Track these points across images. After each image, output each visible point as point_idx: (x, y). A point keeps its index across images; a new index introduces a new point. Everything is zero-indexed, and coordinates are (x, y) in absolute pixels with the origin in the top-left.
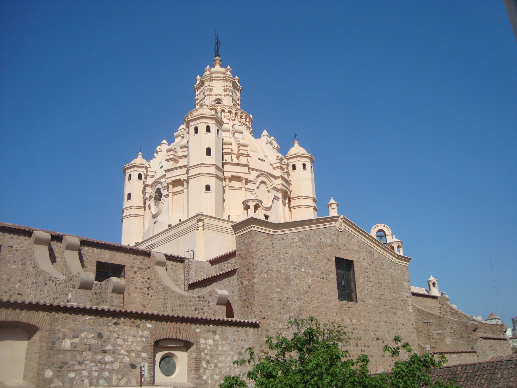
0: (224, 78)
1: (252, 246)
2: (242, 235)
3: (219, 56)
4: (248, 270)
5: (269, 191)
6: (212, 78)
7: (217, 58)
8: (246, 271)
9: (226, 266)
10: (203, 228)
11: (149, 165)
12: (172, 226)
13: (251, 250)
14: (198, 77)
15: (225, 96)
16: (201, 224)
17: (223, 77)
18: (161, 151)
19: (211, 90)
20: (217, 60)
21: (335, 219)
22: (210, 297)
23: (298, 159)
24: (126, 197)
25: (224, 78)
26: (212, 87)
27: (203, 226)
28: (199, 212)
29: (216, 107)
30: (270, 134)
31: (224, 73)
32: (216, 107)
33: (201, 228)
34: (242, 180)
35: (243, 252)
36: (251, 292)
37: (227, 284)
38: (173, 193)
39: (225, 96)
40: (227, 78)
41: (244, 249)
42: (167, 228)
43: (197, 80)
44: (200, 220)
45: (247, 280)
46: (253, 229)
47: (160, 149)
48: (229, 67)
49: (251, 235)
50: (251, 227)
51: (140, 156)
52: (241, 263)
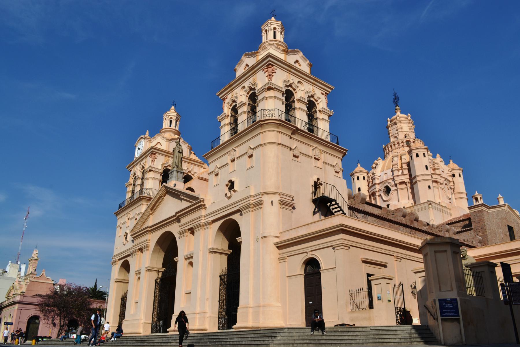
2: (475, 212)
3: (398, 106)
4: (481, 228)
5: (448, 189)
7: (397, 107)
12: (405, 207)
14: (388, 119)
15: (410, 132)
16: (430, 206)
17: (408, 121)
19: (402, 129)
20: (398, 109)
21: (503, 206)
22: (473, 240)
23: (456, 171)
28: (429, 200)
30: (441, 157)
31: (407, 119)
33: (431, 208)
34: (438, 183)
35: (477, 220)
36: (485, 239)
37: (466, 235)
38: (400, 189)
39: (410, 132)
41: (477, 218)
43: (388, 121)
44: (430, 204)
45: (481, 233)
48: (409, 114)
50: (482, 208)
51: (359, 165)
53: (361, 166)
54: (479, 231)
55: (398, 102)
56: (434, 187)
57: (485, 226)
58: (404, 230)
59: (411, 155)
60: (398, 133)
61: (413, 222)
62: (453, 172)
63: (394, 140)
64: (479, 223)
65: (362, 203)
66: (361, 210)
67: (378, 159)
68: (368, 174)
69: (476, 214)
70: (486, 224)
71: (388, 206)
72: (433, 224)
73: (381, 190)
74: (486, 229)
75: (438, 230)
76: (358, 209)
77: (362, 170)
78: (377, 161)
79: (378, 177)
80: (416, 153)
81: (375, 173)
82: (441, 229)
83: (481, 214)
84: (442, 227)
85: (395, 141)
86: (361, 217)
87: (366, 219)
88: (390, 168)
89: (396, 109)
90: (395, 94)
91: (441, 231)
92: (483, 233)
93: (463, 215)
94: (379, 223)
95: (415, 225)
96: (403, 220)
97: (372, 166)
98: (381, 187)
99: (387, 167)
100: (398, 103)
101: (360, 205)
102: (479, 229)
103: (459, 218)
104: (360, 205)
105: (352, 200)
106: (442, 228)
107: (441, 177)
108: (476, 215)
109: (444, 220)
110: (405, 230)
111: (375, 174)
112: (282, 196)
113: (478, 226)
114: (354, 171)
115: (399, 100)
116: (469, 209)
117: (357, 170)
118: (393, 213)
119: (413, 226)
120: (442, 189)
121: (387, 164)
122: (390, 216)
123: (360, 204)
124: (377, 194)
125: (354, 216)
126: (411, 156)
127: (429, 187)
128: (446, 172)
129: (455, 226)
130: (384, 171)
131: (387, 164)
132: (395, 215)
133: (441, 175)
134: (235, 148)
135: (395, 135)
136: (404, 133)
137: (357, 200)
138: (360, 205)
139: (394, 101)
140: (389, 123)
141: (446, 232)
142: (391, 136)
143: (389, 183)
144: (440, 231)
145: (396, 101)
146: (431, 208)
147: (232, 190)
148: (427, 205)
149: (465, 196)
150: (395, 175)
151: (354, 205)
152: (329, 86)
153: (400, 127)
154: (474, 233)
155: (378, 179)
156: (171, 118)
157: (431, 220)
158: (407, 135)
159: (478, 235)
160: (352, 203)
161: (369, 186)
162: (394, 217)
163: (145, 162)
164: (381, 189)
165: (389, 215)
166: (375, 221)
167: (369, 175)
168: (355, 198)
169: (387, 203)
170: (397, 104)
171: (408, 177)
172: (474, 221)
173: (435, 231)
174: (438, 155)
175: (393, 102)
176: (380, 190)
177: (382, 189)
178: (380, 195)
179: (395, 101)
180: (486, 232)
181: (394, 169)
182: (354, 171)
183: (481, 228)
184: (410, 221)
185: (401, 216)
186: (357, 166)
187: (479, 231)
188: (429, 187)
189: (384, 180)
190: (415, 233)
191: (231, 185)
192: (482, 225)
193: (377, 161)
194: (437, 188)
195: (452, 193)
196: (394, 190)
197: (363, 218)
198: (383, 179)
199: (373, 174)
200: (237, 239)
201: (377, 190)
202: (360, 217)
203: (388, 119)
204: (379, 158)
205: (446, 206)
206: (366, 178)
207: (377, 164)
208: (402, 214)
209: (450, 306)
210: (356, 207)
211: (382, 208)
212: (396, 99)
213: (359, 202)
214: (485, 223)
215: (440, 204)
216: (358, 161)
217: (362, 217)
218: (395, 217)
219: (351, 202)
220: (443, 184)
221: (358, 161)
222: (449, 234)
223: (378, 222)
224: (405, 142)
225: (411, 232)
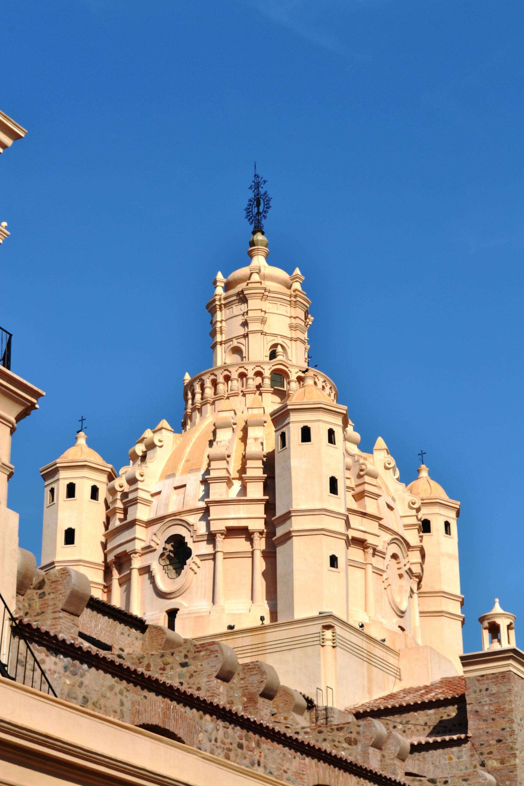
0: (293, 299)
1: (508, 699)
3: (263, 233)
4: (499, 741)
5: (401, 576)
6: (266, 293)
7: (259, 237)
8: (493, 742)
9: (400, 727)
10: (334, 643)
11: (142, 476)
12: (236, 629)
13: (507, 706)
14: (220, 276)
15: (291, 339)
16: (328, 634)
17: (290, 296)
18: (161, 447)
19: (263, 321)
23: (436, 509)
24: (61, 537)
25: (293, 299)
26: (265, 312)
27: (334, 640)
28: (326, 609)
29: (287, 368)
32: (287, 368)
34: (367, 547)
35: (486, 708)
36: (508, 783)
37: (442, 762)
38: (224, 553)
39: (291, 339)
40: (298, 299)
41: (488, 702)
42: (225, 630)
43: (218, 284)
44: (328, 627)
45: (497, 760)
46: (511, 669)
47: (160, 441)
48: (297, 271)
49: (505, 680)
50: (508, 665)
51: (82, 440)
52: (480, 727)
53: (90, 443)
54: (491, 753)
55: (265, 217)
56: (352, 563)
57: (512, 733)
58: (218, 730)
59: (284, 430)
60: (246, 336)
61: (256, 703)
62: (425, 513)
63: (228, 362)
64: (493, 719)
65: (72, 614)
66: (64, 641)
67: (159, 426)
68: (111, 477)
69: (485, 686)
70: (515, 726)
71: (172, 614)
72: (330, 705)
73: (155, 550)
74: (516, 747)
75: (342, 739)
76: (52, 634)
77: (92, 459)
78: (154, 432)
79: (147, 496)
80: (302, 425)
81: (139, 477)
82: (353, 736)
83: (504, 689)
84: (359, 726)
85: (232, 365)
86: (60, 668)
87: (77, 678)
88: (198, 470)
89: (252, 244)
90: (257, 186)
91: (356, 742)
92: (502, 762)
93: (441, 682)
94: (124, 700)
95: (262, 713)
96: (221, 690)
97: (131, 451)
98: (154, 538)
99: (187, 461)
100: (263, 222)
101: (60, 618)
102: (491, 742)
103: (427, 693)
104: (60, 618)
105: (32, 593)
106: (358, 733)
107: (380, 525)
108: (487, 690)
109: (370, 692)
110: (220, 735)
111: (140, 485)
113: (490, 730)
114: (58, 460)
115: (270, 211)
116: (464, 665)
117: (70, 458)
118: (184, 661)
119: (252, 718)
120: (379, 572)
121: (188, 449)
122: (172, 668)
123: (62, 614)
124: (137, 563)
125: (31, 661)
126: (283, 435)
127: (334, 561)
128: (401, 508)
129: (407, 722)
130: (173, 475)
131: (188, 449)
132: (192, 668)
133: (380, 519)
135: (235, 343)
136: (271, 341)
137: (52, 596)
138: (61, 620)
139: (248, 211)
140: (219, 290)
141: (371, 750)
142: (221, 343)
143: (187, 525)
144: (350, 744)
145: (258, 213)
146: (329, 643)
148: (317, 628)
149: (455, 608)
150: (212, 497)
151: (38, 614)
152: (5, 122)
153: (259, 314)
154: (472, 756)
155: (147, 503)
157: (323, 688)
158: (279, 349)
159: (483, 765)
160: (30, 605)
161: (111, 528)
162: (188, 675)
164: (153, 544)
165: (168, 664)
166: (111, 688)
167: (116, 483)
168: (46, 589)
169: (170, 604)
170: (259, 222)
171: (260, 510)
172: (477, 712)
173: (334, 741)
174: (380, 442)
175: (244, 214)
176: (148, 550)
177: (157, 547)
178: (146, 570)
179: (255, 211)
180: (515, 756)
181: (213, 474)
182: (60, 461)
183: (499, 741)
184: (244, 695)
185: (215, 674)
186: (73, 442)
187: (491, 753)
188: (334, 561)
189: (172, 510)
190: (258, 745)
192: (503, 729)
193: (154, 432)
194: (362, 566)
195: (412, 591)
196: (203, 557)
197: (68, 673)
198: (167, 505)
199: (132, 481)
201: (138, 546)
202: (53, 667)
203: (220, 276)
204: (164, 423)
205: (384, 640)
206: (103, 494)
207: (151, 446)
208: (219, 666)
210: (44, 629)
211: (147, 626)
212: (258, 205)
213: (60, 606)
214: (512, 721)
215: (366, 630)
216: (82, 420)
217: (62, 671)
218: (191, 676)
219: (26, 605)
220: (384, 554)
221: (82, 420)
222: (383, 756)
223: (121, 693)
224: (267, 373)
225: (244, 742)
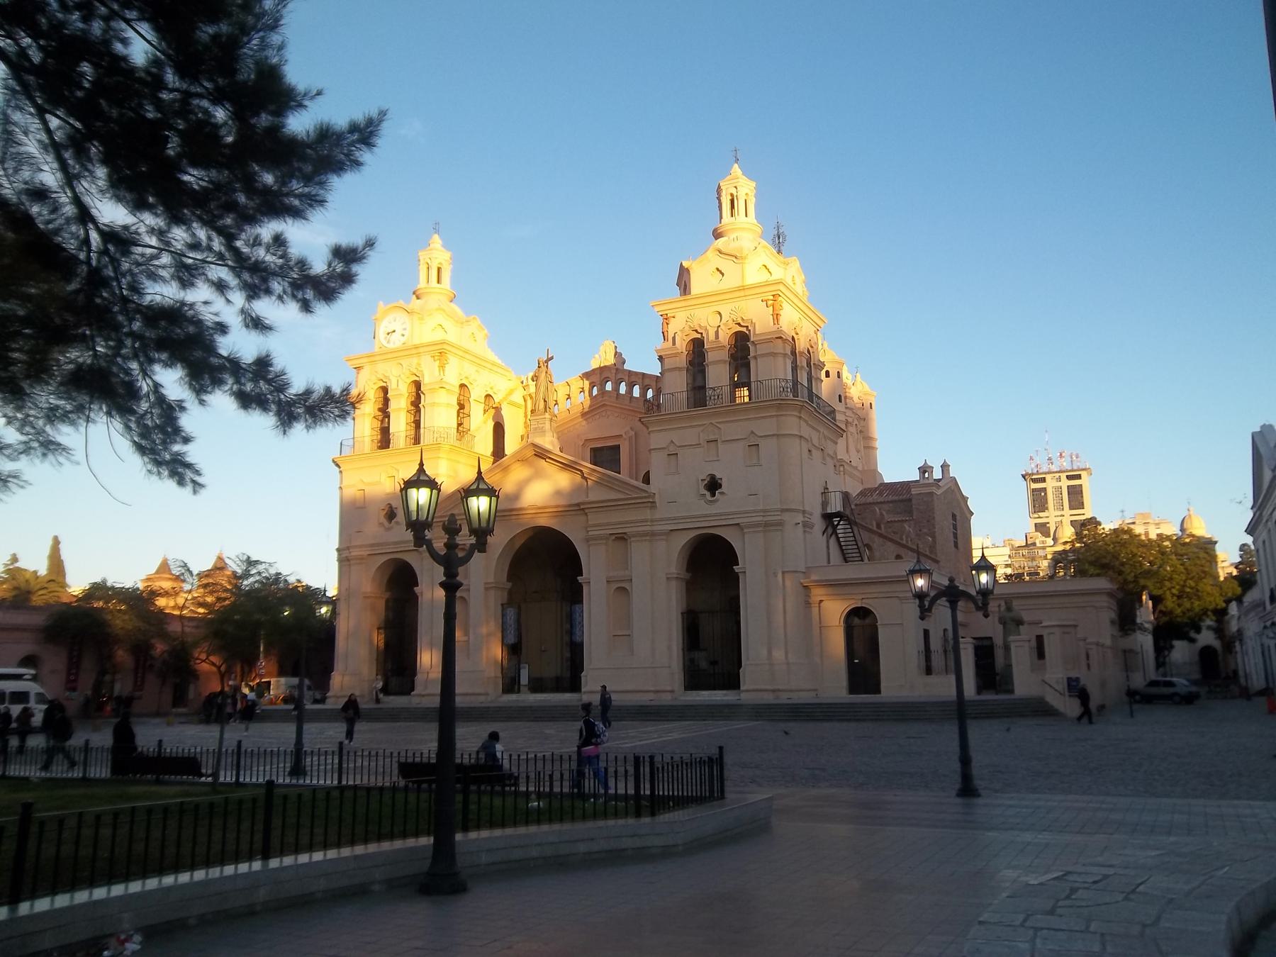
100: (782, 248)
112: (806, 515)
115: (786, 242)
134: (717, 423)
145: (779, 242)
146: (842, 473)
147: (717, 492)
156: (440, 263)
163: (419, 364)
191: (713, 485)
200: (734, 567)
209: (1074, 684)
212: (779, 238)
